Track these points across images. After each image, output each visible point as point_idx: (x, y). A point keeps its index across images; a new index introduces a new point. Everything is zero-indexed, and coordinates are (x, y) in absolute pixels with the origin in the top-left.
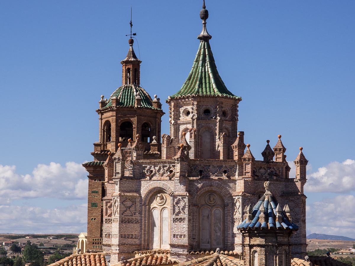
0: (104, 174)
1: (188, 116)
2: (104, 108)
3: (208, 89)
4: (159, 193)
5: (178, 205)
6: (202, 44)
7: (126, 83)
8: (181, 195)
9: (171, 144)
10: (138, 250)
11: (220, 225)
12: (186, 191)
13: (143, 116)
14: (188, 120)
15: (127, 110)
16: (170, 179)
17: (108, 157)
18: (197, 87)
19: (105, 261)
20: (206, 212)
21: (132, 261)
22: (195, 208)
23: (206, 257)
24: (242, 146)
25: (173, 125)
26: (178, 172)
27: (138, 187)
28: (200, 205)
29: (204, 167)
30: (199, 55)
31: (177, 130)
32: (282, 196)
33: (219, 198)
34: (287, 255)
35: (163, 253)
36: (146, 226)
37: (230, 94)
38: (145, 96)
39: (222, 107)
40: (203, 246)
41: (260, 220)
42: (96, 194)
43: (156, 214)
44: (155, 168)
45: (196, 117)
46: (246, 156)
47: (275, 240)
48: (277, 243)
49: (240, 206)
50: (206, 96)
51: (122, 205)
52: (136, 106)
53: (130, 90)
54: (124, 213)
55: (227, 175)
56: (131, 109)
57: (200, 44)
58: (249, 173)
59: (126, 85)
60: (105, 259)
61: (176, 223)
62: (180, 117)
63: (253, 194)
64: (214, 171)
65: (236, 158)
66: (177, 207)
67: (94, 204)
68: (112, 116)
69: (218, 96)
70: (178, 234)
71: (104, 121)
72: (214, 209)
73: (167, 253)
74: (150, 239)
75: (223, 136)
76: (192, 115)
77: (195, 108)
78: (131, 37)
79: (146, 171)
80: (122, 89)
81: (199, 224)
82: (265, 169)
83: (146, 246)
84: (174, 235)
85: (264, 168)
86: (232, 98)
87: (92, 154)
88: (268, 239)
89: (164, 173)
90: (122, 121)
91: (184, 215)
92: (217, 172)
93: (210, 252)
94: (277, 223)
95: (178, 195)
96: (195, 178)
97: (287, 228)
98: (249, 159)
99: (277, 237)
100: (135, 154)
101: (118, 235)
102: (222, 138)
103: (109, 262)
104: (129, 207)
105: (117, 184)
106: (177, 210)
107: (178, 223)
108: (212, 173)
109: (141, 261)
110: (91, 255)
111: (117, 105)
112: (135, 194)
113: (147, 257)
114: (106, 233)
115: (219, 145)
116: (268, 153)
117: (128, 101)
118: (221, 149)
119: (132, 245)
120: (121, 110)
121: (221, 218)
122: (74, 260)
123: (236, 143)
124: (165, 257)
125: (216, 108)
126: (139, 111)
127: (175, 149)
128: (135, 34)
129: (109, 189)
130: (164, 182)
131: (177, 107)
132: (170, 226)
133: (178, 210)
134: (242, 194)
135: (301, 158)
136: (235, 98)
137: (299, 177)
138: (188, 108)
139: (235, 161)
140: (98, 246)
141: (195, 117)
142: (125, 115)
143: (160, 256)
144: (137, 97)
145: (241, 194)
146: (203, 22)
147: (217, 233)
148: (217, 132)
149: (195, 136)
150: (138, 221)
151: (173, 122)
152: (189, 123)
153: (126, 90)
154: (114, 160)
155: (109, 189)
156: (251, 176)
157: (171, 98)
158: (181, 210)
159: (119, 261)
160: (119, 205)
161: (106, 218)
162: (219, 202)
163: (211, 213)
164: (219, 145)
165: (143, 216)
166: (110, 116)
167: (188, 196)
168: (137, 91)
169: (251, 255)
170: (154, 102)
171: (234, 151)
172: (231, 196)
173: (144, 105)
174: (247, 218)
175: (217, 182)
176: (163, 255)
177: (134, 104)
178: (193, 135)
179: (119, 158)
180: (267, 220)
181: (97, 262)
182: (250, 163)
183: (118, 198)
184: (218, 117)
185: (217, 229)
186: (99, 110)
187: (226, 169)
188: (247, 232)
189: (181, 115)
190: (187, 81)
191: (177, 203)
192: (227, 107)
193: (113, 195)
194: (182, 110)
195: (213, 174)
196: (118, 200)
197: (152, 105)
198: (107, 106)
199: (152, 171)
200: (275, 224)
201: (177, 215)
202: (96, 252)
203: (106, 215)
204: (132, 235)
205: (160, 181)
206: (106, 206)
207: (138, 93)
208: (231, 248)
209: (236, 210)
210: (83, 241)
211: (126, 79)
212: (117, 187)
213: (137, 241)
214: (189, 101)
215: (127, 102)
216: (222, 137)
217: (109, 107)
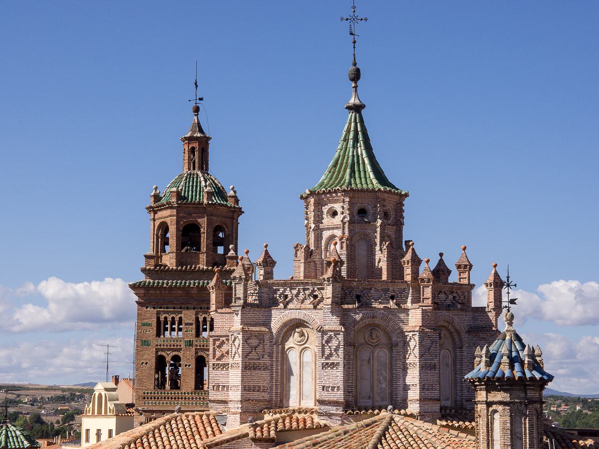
0: (209, 301)
1: (334, 218)
2: (157, 204)
3: (363, 180)
4: (298, 327)
5: (329, 345)
6: (351, 115)
7: (189, 169)
8: (334, 331)
9: (310, 258)
10: (268, 408)
11: (386, 373)
12: (340, 325)
13: (215, 216)
14: (336, 224)
16: (315, 308)
17: (216, 275)
18: (347, 177)
19: (218, 424)
20: (365, 354)
21: (264, 424)
22: (351, 349)
23: (373, 419)
24: (416, 261)
26: (330, 298)
28: (357, 344)
30: (348, 131)
31: (318, 238)
32: (469, 332)
33: (383, 334)
34: (538, 416)
35: (306, 413)
36: (279, 374)
37: (393, 187)
38: (216, 187)
39: (384, 206)
40: (362, 402)
41: (501, 366)
42: (147, 327)
43: (293, 357)
44: (291, 292)
45: (349, 219)
46: (424, 276)
47: (524, 395)
48: (527, 399)
49: (416, 346)
50: (362, 190)
51: (245, 344)
53: (195, 179)
54: (248, 355)
55: (396, 301)
56: (198, 206)
57: (348, 116)
58: (429, 299)
59: (189, 172)
60: (217, 421)
61: (327, 371)
62: (323, 218)
63: (434, 330)
64: (377, 296)
65: (408, 278)
66: (328, 347)
67: (145, 341)
68: (171, 216)
69: (379, 190)
70: (328, 385)
71: (157, 223)
72: (378, 351)
73: (312, 413)
74: (285, 393)
75: (387, 247)
76: (342, 216)
77: (346, 206)
78: (196, 103)
79: (278, 295)
80: (183, 177)
81: (357, 372)
83: (279, 402)
84: (323, 387)
85: (444, 292)
86: (398, 192)
87: (141, 271)
88: (513, 394)
89: (305, 299)
90: (184, 222)
91: (337, 359)
92: (382, 298)
93: (373, 410)
94: (527, 371)
95: (329, 331)
96: (350, 306)
97: (541, 379)
98: (429, 279)
100: (263, 271)
101: (241, 386)
102: (385, 249)
103: (225, 425)
104: (256, 347)
105: (237, 315)
106: (327, 352)
108: (374, 299)
109: (276, 425)
110: (196, 415)
111: (178, 200)
112: (263, 329)
113: (284, 419)
114: (214, 384)
116: (441, 272)
117: (194, 194)
118: (383, 265)
119: (259, 401)
121: (388, 363)
122: (173, 422)
123: (408, 256)
124: (310, 419)
125: (376, 206)
127: (316, 264)
128: (201, 99)
129: (217, 321)
130: (306, 312)
131: (319, 205)
132: (314, 375)
133: (330, 352)
134: (420, 329)
135: (495, 279)
136: (401, 193)
137: (492, 305)
138: (336, 206)
139: (406, 282)
140: (150, 402)
141: (346, 219)
142: (190, 214)
143: (301, 416)
144: (207, 188)
145: (417, 329)
147: (381, 384)
148: (378, 241)
149: (347, 245)
150: (267, 367)
151: (313, 226)
152: (337, 228)
153: (190, 178)
154: (233, 280)
155: (217, 321)
156: (432, 303)
157: (311, 192)
158: (332, 351)
159: (241, 423)
160: (241, 345)
161: (213, 363)
162: (384, 340)
163: (373, 356)
165: (274, 359)
166: (168, 216)
167: (342, 332)
168: (206, 181)
169: (490, 417)
170: (230, 196)
171: (405, 268)
172: (402, 332)
173: (216, 200)
174: (483, 364)
175: (382, 311)
176: (306, 416)
177: (203, 199)
178: (344, 245)
179: (240, 277)
180: (512, 367)
181: (206, 426)
183: (239, 334)
184: (378, 220)
185: (381, 378)
186: (151, 207)
187: (393, 294)
188: (483, 383)
189: (324, 216)
190: (331, 169)
191: (328, 342)
192: (390, 207)
193: (231, 330)
194: (325, 209)
195: (376, 300)
196: (240, 336)
197: (227, 201)
198: (163, 201)
199: (286, 296)
200: (524, 373)
201: (328, 358)
202: (203, 411)
203: (214, 358)
204: (259, 387)
205: (299, 311)
206: (214, 345)
207: (207, 183)
208: (401, 405)
209: (409, 352)
210: (100, 395)
211: (189, 163)
212: (237, 319)
213: (266, 396)
216: (385, 247)
217: (167, 203)
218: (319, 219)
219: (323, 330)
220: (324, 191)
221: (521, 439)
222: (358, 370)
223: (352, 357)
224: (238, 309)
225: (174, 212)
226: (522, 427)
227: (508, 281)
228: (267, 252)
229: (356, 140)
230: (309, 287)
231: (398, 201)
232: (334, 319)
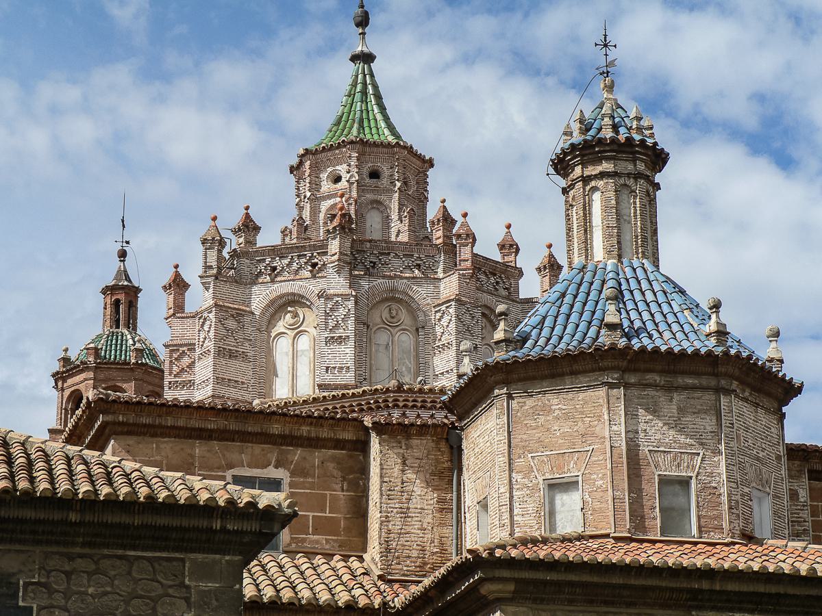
2: (67, 370)
7: (111, 327)
9: (305, 232)
11: (410, 362)
12: (350, 288)
15: (115, 368)
20: (382, 338)
25: (308, 199)
27: (249, 297)
29: (378, 257)
43: (282, 349)
45: (357, 178)
52: (133, 361)
56: (123, 367)
58: (467, 260)
61: (332, 347)
68: (85, 380)
70: (334, 365)
71: (67, 393)
72: (398, 334)
76: (349, 175)
82: (487, 275)
84: (327, 368)
95: (335, 295)
98: (468, 235)
99: (636, 160)
102: (405, 217)
106: (331, 324)
107: (336, 347)
115: (399, 230)
120: (105, 368)
126: (139, 370)
130: (301, 283)
131: (316, 169)
132: (312, 365)
133: (336, 323)
138: (339, 169)
141: (354, 179)
146: (361, 31)
153: (113, 336)
158: (340, 322)
161: (170, 380)
164: (399, 230)
169: (587, 197)
171: (434, 231)
182: (470, 242)
185: (404, 369)
186: (58, 373)
191: (331, 309)
194: (324, 176)
196: (212, 316)
199: (274, 269)
214: (341, 153)
215: (116, 356)
216: (406, 214)
218: (315, 186)
219: (327, 295)
220: (324, 147)
221: (629, 222)
222: (373, 358)
223: (365, 340)
224: (210, 280)
225: (91, 374)
226: (630, 208)
227: (605, 41)
228: (247, 214)
229: (364, 93)
230: (306, 253)
231: (421, 170)
232: (342, 281)
